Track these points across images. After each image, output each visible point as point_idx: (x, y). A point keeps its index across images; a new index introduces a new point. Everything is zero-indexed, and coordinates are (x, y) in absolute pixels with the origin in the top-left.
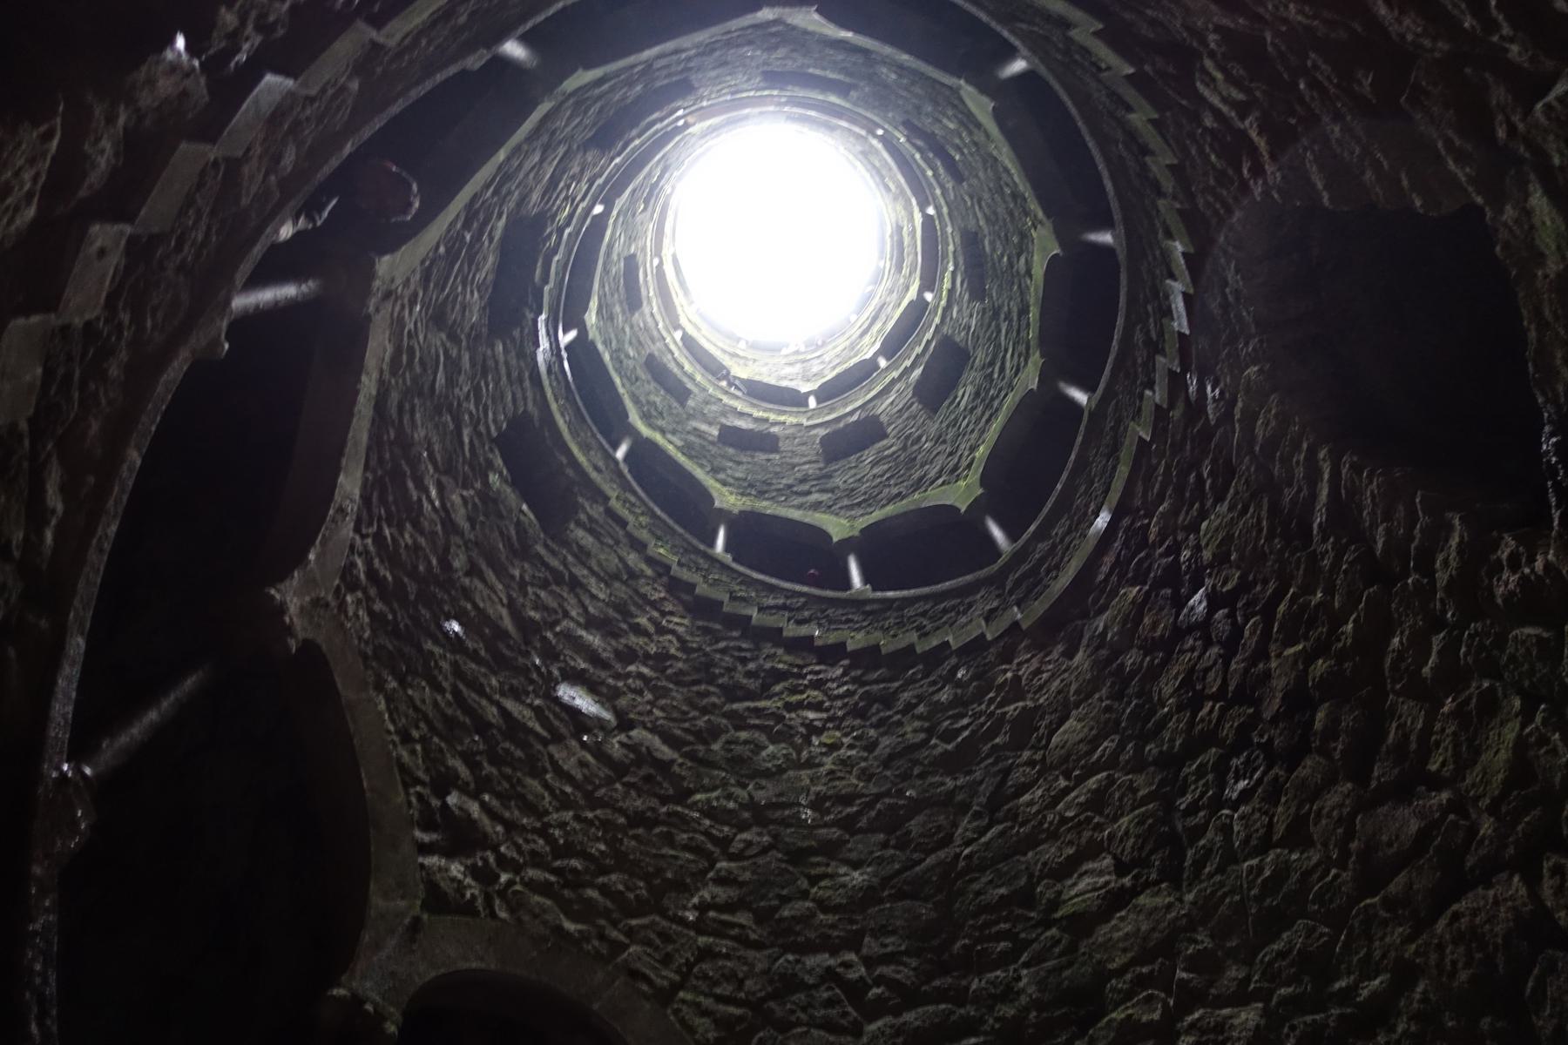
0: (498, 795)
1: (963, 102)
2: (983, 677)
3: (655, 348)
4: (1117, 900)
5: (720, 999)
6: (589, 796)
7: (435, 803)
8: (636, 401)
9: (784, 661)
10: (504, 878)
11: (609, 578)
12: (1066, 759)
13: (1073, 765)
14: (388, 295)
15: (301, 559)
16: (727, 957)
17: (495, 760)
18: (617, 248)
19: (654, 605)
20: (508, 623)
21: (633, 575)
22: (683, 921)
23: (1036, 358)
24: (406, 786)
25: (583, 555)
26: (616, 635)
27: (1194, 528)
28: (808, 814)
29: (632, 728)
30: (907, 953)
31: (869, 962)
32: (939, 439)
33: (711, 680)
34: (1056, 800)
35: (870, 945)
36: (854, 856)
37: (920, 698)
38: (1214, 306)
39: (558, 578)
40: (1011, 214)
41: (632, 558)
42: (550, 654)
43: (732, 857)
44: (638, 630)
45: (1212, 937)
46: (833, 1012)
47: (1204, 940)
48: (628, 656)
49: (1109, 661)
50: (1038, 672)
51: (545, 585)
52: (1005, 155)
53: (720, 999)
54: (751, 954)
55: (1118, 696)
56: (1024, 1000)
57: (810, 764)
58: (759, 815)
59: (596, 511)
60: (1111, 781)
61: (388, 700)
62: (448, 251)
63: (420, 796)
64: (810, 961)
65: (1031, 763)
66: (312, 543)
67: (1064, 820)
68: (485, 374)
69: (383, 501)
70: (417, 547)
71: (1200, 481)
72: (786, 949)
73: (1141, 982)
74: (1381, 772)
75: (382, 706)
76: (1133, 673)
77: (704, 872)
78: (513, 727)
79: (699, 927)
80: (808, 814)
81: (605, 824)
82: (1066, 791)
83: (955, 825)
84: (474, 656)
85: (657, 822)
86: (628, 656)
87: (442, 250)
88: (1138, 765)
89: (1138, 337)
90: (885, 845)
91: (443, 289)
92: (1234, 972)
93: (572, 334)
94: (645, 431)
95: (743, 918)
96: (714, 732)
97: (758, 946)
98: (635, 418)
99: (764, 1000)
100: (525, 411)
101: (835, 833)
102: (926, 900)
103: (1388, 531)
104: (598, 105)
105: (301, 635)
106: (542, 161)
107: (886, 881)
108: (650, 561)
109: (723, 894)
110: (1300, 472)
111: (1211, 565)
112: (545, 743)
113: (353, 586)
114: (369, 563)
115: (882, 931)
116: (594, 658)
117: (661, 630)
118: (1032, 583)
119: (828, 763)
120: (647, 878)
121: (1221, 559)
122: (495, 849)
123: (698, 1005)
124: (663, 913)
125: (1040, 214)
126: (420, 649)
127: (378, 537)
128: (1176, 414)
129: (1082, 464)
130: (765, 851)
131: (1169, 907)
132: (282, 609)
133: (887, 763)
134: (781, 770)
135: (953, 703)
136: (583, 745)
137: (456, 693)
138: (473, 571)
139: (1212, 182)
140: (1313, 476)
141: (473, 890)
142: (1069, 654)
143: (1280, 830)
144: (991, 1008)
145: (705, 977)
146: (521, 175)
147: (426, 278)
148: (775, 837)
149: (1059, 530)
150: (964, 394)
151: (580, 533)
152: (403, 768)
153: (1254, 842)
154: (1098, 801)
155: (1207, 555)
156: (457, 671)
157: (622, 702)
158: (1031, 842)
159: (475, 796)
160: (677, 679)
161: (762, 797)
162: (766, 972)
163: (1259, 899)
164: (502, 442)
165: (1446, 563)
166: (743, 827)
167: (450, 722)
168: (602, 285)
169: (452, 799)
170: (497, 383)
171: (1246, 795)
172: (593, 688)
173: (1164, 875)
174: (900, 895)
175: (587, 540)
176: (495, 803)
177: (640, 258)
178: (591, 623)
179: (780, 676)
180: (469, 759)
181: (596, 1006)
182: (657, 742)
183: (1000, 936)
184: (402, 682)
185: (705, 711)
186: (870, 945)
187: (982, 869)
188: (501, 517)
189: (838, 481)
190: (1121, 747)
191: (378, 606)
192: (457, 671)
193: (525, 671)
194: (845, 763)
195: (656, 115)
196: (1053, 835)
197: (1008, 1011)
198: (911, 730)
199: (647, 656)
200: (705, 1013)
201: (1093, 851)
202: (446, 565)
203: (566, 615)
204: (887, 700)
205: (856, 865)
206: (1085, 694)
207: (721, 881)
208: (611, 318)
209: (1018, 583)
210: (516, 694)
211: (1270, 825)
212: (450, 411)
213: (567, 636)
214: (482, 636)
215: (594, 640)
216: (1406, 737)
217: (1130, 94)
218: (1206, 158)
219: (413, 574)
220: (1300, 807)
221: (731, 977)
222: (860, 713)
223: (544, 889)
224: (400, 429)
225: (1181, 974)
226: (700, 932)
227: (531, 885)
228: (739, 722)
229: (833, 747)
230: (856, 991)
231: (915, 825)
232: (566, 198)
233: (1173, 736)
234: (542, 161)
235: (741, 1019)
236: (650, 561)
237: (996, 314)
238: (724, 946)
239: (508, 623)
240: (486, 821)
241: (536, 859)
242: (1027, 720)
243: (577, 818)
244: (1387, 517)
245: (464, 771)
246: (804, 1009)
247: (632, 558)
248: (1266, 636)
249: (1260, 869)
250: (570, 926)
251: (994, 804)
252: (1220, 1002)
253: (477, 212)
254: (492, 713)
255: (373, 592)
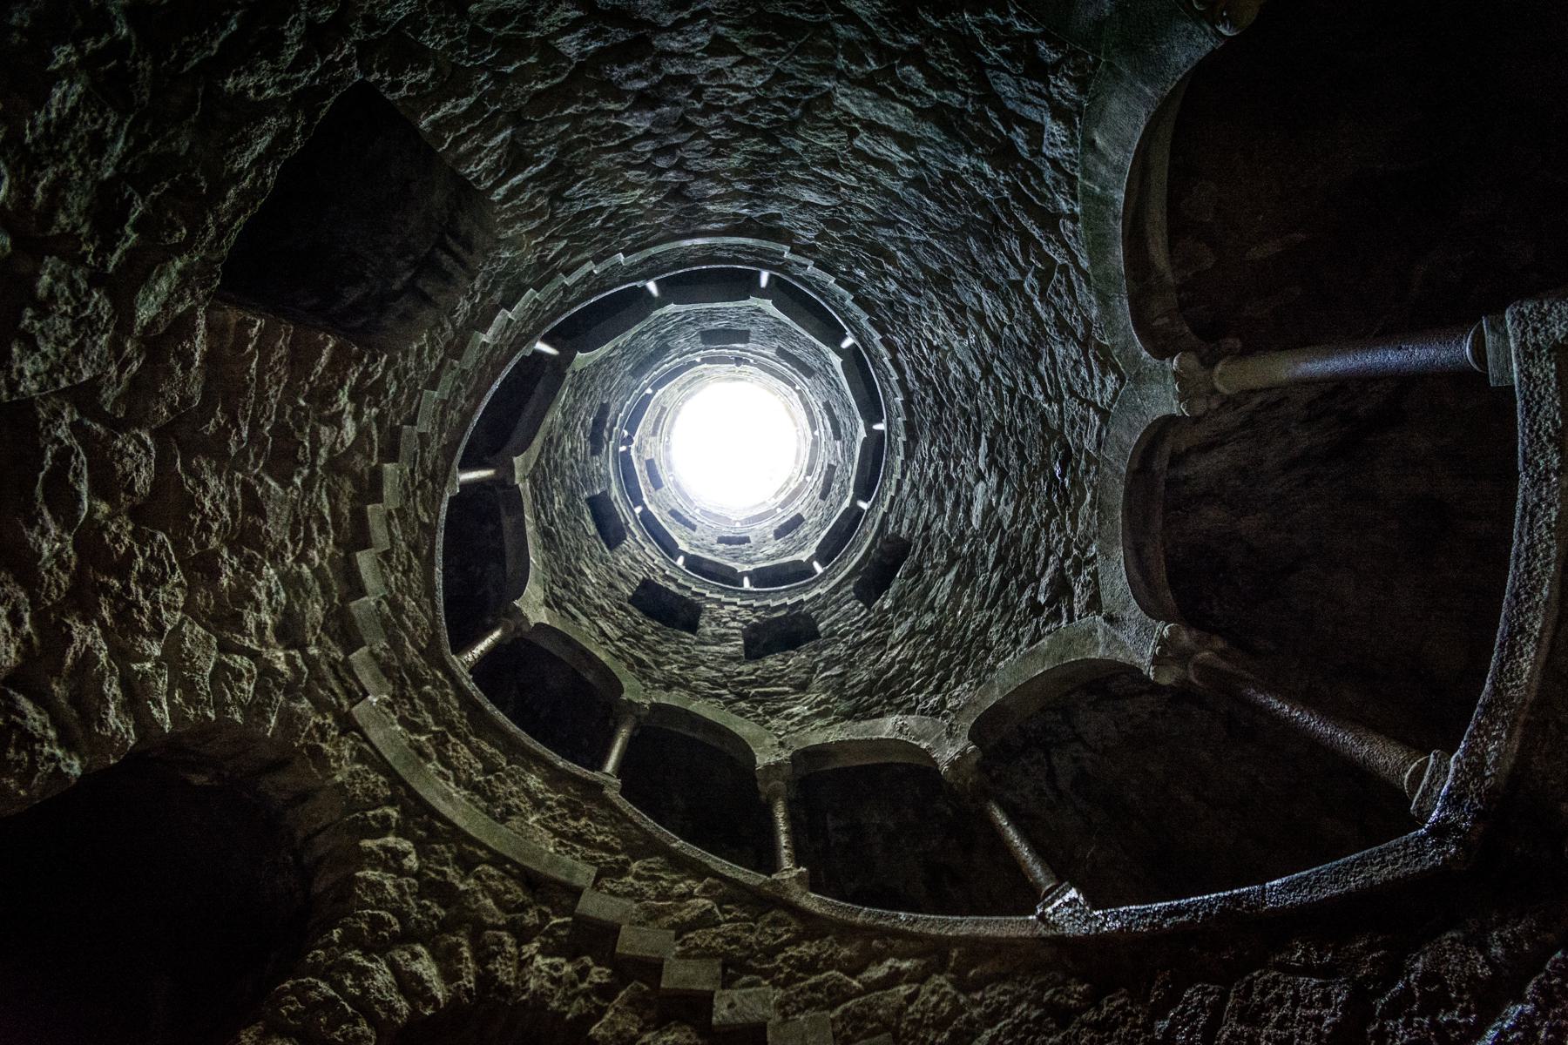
0: (1035, 564)
1: (537, 464)
2: (837, 255)
3: (817, 494)
4: (872, 127)
5: (1091, 376)
6: (1021, 495)
7: (1046, 614)
8: (840, 503)
9: (909, 375)
10: (1075, 552)
11: (920, 503)
12: (829, 193)
13: (832, 188)
14: (782, 744)
15: (926, 753)
16: (1066, 376)
17: (1018, 569)
18: (771, 551)
19: (922, 468)
20: (951, 576)
21: (914, 486)
22: (1061, 412)
23: (658, 313)
24: (1040, 638)
25: (913, 526)
26: (943, 491)
27: (635, 204)
28: (972, 336)
29: (979, 471)
30: (1002, 247)
31: (1023, 273)
32: (753, 322)
33: (940, 420)
34: (854, 189)
35: (1014, 275)
36: (974, 300)
37: (874, 287)
38: (498, 296)
39: (926, 540)
40: (593, 379)
41: (906, 488)
42: (961, 538)
43: (1016, 384)
44: (936, 476)
45: (835, 57)
46: (1062, 290)
47: (841, 62)
48: (948, 477)
49: (758, 197)
50: (803, 228)
51: (931, 549)
52: (555, 416)
53: (1091, 376)
54: (1059, 360)
55: (769, 182)
56: (974, 161)
57: (948, 344)
58: (987, 371)
59: (892, 518)
60: (814, 164)
61: (998, 660)
62: (761, 702)
63: (1045, 624)
64: (1044, 316)
65: (850, 211)
66: (918, 747)
67: (860, 180)
68: (833, 633)
69: (898, 693)
70: (922, 657)
71: (605, 221)
72: (1045, 333)
73: (902, 89)
74: (621, 36)
75: (1001, 664)
76: (750, 182)
77: (1031, 403)
78: (1000, 559)
79: (1060, 400)
80: (972, 336)
81: (1031, 481)
82: (845, 186)
83: (918, 242)
84: (971, 596)
85: (1018, 442)
86: (948, 477)
87: (760, 711)
88: (791, 153)
89: (571, 298)
90: (958, 283)
91: (787, 693)
92: (841, 31)
93: (816, 565)
94: (851, 493)
95: (1042, 369)
96: (963, 411)
97: (1052, 354)
98: (847, 503)
99: (1079, 343)
100: (854, 590)
101: (970, 317)
102: (967, 246)
103: (487, 140)
104: (660, 648)
105: (967, 742)
106: (703, 663)
107: (976, 276)
108: (904, 475)
109: (1037, 387)
110: (527, 196)
111: (641, 186)
112: (1004, 532)
113: (943, 703)
114: (932, 694)
115: (1000, 268)
116: (956, 504)
117: (931, 460)
118: (761, 252)
119: (940, 332)
120: (1047, 444)
121: (635, 186)
122: (1062, 561)
123: (1101, 391)
124: (1061, 427)
125: (569, 375)
126: (973, 640)
127: (919, 690)
128: (587, 255)
129: (678, 265)
130: (1002, 362)
131: (845, 95)
132: (953, 764)
133: (919, 295)
134: (960, 362)
135: (863, 268)
136: (998, 503)
137: (990, 607)
138: (931, 608)
139: (412, 373)
140: (514, 192)
141: (1085, 576)
142: (779, 217)
143: (731, 59)
144: (995, 181)
145: (1083, 388)
146: (714, 673)
147: (774, 713)
148: (993, 357)
149: (726, 254)
150: (721, 324)
151: (904, 530)
152: (1031, 643)
153: (756, 68)
154: (833, 164)
155: (639, 192)
156: (980, 608)
157: (971, 480)
158: (888, 193)
159: (1038, 580)
160: (948, 442)
161: (978, 372)
162: (1063, 344)
163: (784, 45)
164: (868, 605)
165: (455, 107)
166: (997, 379)
167: (1006, 608)
168: (789, 553)
169: (1042, 599)
170: (837, 621)
171: (738, 88)
172: (970, 503)
173: (830, 108)
174: (975, 263)
175: (906, 522)
176: (1038, 567)
177: (776, 526)
178: (942, 511)
179: (919, 376)
180: (1021, 588)
181: (1124, 470)
182: (981, 450)
183: (953, 192)
184: (988, 650)
185: (955, 421)
186: (1014, 275)
187: (926, 217)
188: (903, 595)
189: (817, 364)
190: (791, 167)
191: (952, 681)
192: (980, 608)
193: (972, 555)
194: (934, 319)
195: (673, 587)
196: (874, 182)
197: (986, 168)
198: (893, 287)
199: (946, 467)
200: (1104, 385)
201: (858, 153)
202: (930, 630)
203: (941, 531)
204: (890, 304)
205: (979, 299)
206: (789, 200)
207: (1030, 388)
208: (805, 537)
209: (773, 259)
210: (985, 560)
211: (735, 65)
212: (852, 655)
213: (951, 527)
214: (961, 592)
215: (948, 504)
216: (584, 39)
217: (409, 445)
218: (400, 390)
219: (935, 655)
220: (702, 58)
221: (1075, 369)
222: (906, 316)
223: (1074, 518)
224: (861, 693)
225: (874, 66)
226: (1062, 398)
227: (1074, 529)
228: (951, 395)
229: (932, 331)
230: (1044, 277)
231: (936, 266)
232: (734, 620)
233: (754, 144)
234: (703, 663)
235: (1096, 357)
236: (904, 475)
237: (663, 337)
238: (1062, 380)
239: (951, 576)
240: (1050, 570)
241: (1061, 528)
242: (832, 223)
243: (1033, 501)
244: (479, 149)
245: (1028, 593)
246: (1070, 312)
247: (906, 488)
248: (637, 139)
249: (765, 55)
250: (1089, 496)
251: (890, 224)
252: (866, 30)
253: (737, 694)
254: (996, 578)
255: (946, 686)
